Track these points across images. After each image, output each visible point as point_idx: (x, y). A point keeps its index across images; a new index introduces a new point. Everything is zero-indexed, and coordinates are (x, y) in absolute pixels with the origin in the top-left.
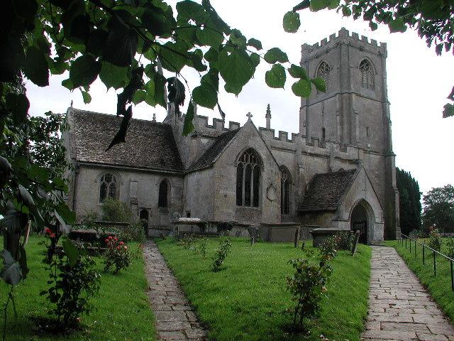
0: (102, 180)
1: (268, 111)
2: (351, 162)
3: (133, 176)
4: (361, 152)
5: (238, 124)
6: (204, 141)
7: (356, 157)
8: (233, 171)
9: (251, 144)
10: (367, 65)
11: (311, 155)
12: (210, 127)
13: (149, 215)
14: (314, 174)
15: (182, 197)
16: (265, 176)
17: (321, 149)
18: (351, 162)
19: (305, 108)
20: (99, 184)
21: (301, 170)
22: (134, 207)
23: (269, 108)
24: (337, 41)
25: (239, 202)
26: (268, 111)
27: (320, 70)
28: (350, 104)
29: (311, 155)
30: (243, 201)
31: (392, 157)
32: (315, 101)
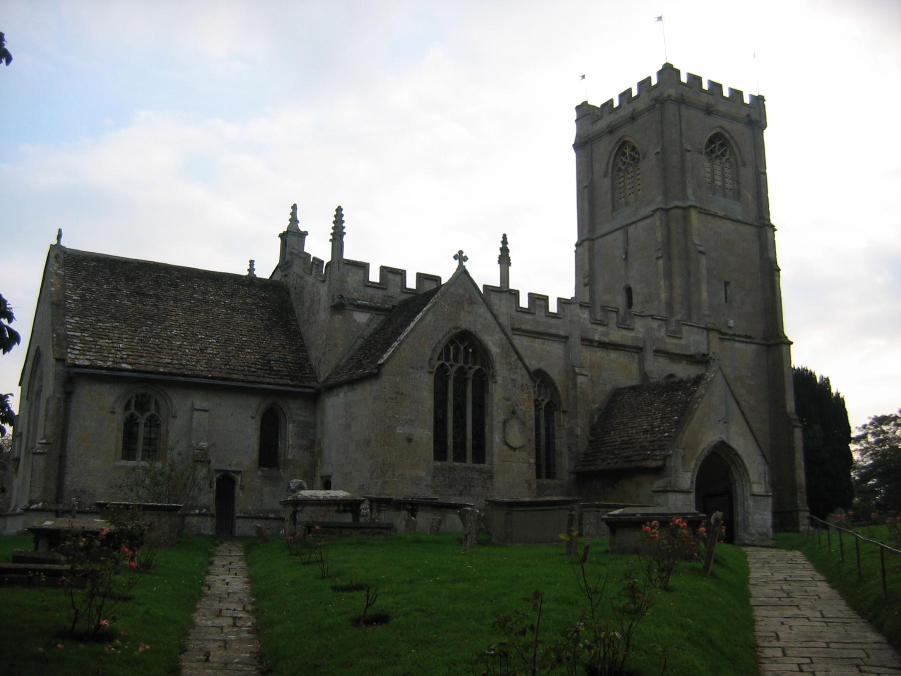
0: (127, 407)
1: (505, 251)
2: (692, 359)
3: (200, 401)
4: (714, 336)
5: (437, 279)
6: (361, 317)
7: (703, 349)
8: (426, 381)
9: (466, 322)
10: (722, 145)
11: (603, 345)
12: (373, 285)
13: (238, 487)
14: (608, 388)
15: (313, 447)
16: (497, 393)
17: (625, 332)
18: (692, 359)
19: (586, 244)
20: (119, 418)
21: (580, 379)
22: (202, 472)
23: (505, 241)
24: (654, 94)
25: (440, 453)
26: (505, 251)
27: (618, 160)
28: (686, 232)
29: (603, 345)
30: (450, 451)
31: (784, 347)
32: (608, 228)
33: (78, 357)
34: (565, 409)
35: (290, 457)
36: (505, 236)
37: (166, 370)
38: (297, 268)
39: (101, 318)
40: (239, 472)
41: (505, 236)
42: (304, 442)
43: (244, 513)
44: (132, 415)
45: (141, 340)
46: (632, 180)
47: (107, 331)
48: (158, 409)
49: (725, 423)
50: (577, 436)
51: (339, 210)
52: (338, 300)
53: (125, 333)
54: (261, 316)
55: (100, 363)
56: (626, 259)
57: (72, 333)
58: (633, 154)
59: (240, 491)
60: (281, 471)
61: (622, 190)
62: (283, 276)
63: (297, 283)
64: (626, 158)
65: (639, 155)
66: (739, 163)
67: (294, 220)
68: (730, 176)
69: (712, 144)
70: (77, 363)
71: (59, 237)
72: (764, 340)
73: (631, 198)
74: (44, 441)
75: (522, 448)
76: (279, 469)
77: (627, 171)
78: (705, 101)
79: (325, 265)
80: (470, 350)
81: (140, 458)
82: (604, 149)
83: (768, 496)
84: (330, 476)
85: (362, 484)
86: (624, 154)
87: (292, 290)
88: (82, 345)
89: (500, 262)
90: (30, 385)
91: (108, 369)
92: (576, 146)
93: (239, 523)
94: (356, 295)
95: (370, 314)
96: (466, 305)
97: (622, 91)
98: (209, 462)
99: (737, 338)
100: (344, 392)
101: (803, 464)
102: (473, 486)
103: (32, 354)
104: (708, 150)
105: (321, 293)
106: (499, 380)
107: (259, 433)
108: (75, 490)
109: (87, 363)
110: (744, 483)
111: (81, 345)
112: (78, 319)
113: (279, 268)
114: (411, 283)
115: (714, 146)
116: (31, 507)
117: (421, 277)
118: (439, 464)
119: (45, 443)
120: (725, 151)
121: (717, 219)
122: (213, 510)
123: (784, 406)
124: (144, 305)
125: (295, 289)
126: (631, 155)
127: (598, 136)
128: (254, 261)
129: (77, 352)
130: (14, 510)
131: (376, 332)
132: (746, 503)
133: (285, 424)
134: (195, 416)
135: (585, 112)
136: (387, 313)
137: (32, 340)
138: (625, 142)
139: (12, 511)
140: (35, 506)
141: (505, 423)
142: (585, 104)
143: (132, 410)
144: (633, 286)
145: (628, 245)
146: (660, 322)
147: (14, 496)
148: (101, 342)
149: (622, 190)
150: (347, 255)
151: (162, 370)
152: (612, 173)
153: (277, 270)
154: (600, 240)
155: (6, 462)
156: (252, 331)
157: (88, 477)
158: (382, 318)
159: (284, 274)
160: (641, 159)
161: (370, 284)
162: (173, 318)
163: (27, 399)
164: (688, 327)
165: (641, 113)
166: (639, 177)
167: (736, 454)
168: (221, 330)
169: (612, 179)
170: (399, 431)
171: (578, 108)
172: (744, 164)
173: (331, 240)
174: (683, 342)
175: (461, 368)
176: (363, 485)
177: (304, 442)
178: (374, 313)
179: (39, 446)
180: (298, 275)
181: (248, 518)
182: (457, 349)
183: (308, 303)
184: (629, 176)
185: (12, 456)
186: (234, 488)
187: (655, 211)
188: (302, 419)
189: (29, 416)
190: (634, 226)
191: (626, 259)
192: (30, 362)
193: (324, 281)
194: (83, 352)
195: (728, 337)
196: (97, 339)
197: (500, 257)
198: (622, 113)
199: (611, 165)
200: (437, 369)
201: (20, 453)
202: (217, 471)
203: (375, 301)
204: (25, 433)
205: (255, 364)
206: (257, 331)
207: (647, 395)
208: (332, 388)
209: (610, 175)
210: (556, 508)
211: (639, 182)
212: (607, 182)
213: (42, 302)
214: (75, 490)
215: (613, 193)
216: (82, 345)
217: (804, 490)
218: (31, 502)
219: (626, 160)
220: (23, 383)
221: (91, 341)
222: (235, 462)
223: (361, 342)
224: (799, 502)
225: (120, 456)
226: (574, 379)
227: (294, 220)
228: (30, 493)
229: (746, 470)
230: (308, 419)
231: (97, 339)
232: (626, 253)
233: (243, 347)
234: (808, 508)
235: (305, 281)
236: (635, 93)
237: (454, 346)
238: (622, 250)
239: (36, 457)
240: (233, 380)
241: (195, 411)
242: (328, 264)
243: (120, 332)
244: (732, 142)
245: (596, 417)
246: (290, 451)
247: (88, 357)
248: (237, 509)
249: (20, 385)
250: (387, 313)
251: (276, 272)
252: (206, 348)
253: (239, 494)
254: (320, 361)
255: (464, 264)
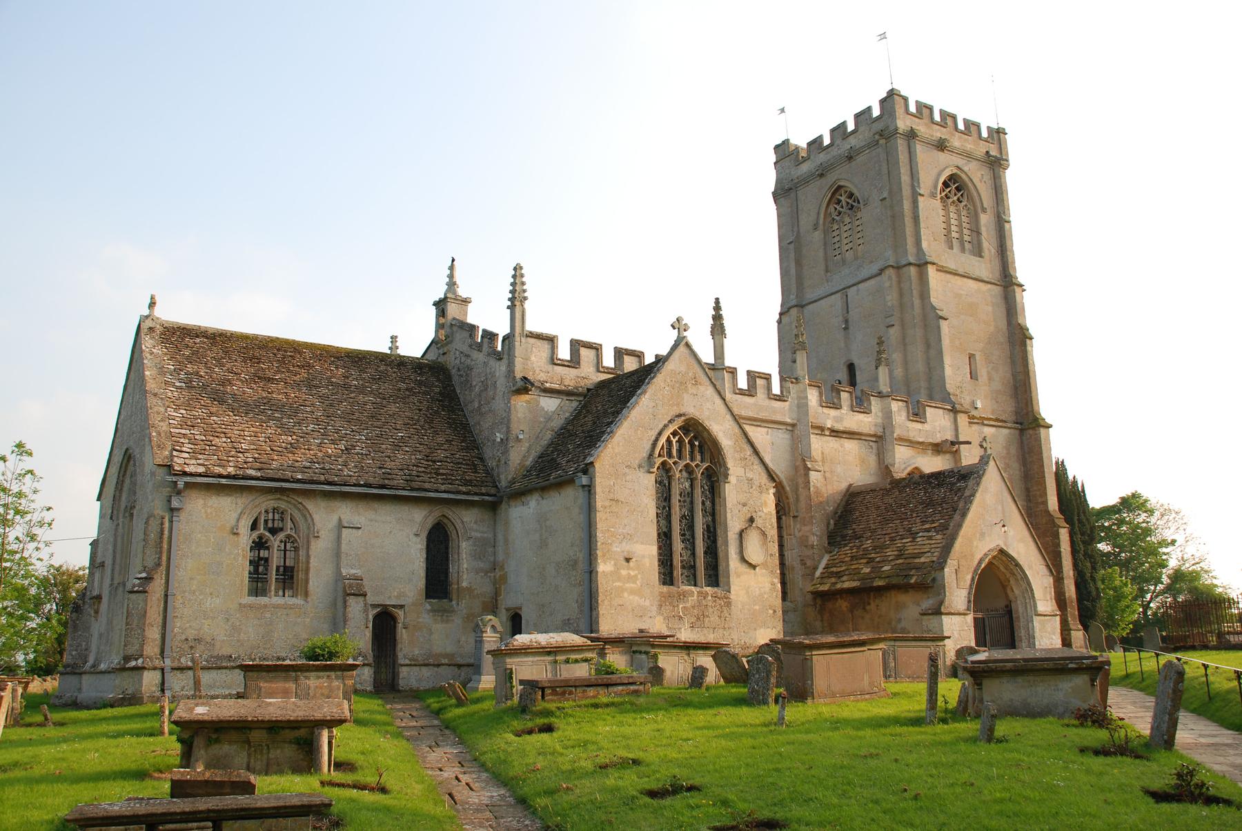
0: (254, 527)
1: (717, 318)
2: (937, 448)
3: (346, 511)
4: (962, 419)
5: (639, 355)
6: (550, 404)
7: (949, 436)
8: (646, 484)
9: (691, 408)
10: (958, 189)
11: (835, 433)
12: (563, 364)
13: (400, 625)
14: (843, 486)
15: (496, 572)
16: (732, 492)
17: (861, 416)
18: (937, 448)
19: (794, 311)
20: (246, 538)
21: (813, 475)
22: (355, 606)
23: (717, 307)
24: (878, 126)
25: (667, 577)
26: (717, 318)
27: (831, 208)
28: (924, 294)
29: (835, 433)
30: (678, 572)
31: (1042, 431)
32: (820, 292)
33: (187, 461)
34: (796, 514)
35: (464, 584)
36: (717, 301)
37: (306, 476)
38: (460, 343)
39: (214, 410)
40: (402, 607)
41: (717, 301)
42: (482, 565)
43: (410, 660)
44: (260, 537)
45: (269, 438)
46: (849, 233)
47: (223, 426)
48: (295, 526)
49: (1004, 526)
50: (812, 547)
51: (517, 268)
52: (522, 383)
53: (247, 429)
54: (419, 404)
55: (218, 470)
56: (846, 328)
57: (177, 431)
58: (850, 201)
59: (404, 630)
60: (454, 602)
61: (837, 246)
62: (439, 354)
63: (461, 363)
64: (842, 207)
65: (859, 202)
66: (979, 210)
67: (452, 284)
68: (968, 226)
69: (947, 188)
70: (187, 470)
71: (152, 304)
72: (1017, 423)
73: (849, 256)
74: (144, 575)
75: (765, 565)
76: (451, 600)
77: (843, 222)
78: (939, 135)
79: (500, 339)
80: (697, 443)
81: (273, 593)
82: (813, 199)
83: (1057, 615)
84: (520, 609)
85: (567, 618)
86: (839, 202)
87: (454, 372)
88: (192, 447)
89: (713, 333)
90: (116, 499)
91: (228, 477)
92: (776, 195)
93: (404, 671)
94: (542, 377)
95: (560, 400)
96: (690, 386)
97: (835, 125)
98: (365, 595)
99: (985, 422)
100: (537, 500)
101: (1071, 573)
102: (707, 616)
103: (118, 458)
104: (943, 194)
105: (497, 375)
106: (732, 479)
107: (425, 556)
108: (187, 640)
109: (201, 470)
110: (1027, 601)
111: (190, 446)
112: (184, 412)
113: (434, 344)
114: (609, 361)
115: (949, 189)
116: (127, 666)
117: (620, 353)
118: (665, 589)
119: (145, 578)
120: (962, 195)
121: (956, 277)
122: (371, 660)
123: (1045, 503)
124: (269, 393)
125: (459, 370)
126: (848, 203)
127: (805, 181)
128: (396, 337)
129: (186, 455)
130: (94, 666)
131: (570, 422)
132: (1030, 625)
133: (457, 543)
134: (343, 536)
135: (784, 152)
136: (581, 399)
137: (117, 440)
138: (840, 187)
139: (91, 668)
140: (133, 663)
141: (741, 534)
142: (786, 143)
143: (261, 530)
144: (856, 362)
145: (848, 312)
146: (900, 403)
147: (94, 648)
148: (216, 441)
149: (837, 246)
150: (531, 326)
151: (300, 477)
152: (824, 224)
153: (432, 347)
154: (810, 307)
155: (80, 602)
156: (408, 424)
157: (204, 621)
158: (575, 404)
159: (441, 351)
160: (862, 207)
161: (559, 362)
162: (308, 409)
163: (111, 518)
164: (932, 409)
165: (859, 151)
166: (859, 229)
167: (1017, 565)
168: (370, 423)
169: (825, 232)
170: (615, 549)
171: (777, 148)
172: (984, 210)
173: (508, 307)
174: (926, 427)
175: (687, 466)
176: (568, 620)
177: (482, 565)
178: (565, 398)
179: (137, 582)
180: (462, 353)
181: (415, 665)
182: (680, 441)
183: (477, 387)
184: (846, 228)
185: (88, 593)
186: (395, 627)
187: (881, 271)
188: (479, 535)
189: (115, 540)
190: (855, 288)
191: (846, 328)
192: (114, 470)
193: (501, 359)
194: (194, 454)
195: (975, 421)
196: (211, 438)
197: (713, 327)
198: (834, 152)
199: (822, 216)
200: (658, 468)
201: (101, 588)
202: (374, 606)
203: (566, 384)
204: (108, 562)
205: (418, 466)
206: (415, 424)
207: (897, 493)
208: (520, 494)
209: (821, 227)
210: (865, 648)
211: (859, 235)
212: (818, 235)
213: (130, 390)
214: (187, 640)
215: (825, 249)
216: (192, 447)
217: (1075, 604)
218: (127, 659)
219: (841, 209)
220: (103, 496)
221: (203, 441)
222: (396, 593)
223: (550, 436)
224: (1069, 619)
225: (246, 591)
226: (807, 475)
227: (452, 284)
228: (125, 646)
229: (1029, 584)
230: (486, 535)
231: (211, 438)
232: (846, 321)
233: (401, 444)
234: (1080, 627)
235: (472, 360)
236: (851, 127)
237: (677, 438)
238: (841, 318)
239: (133, 596)
240: (426, 490)
241: (344, 529)
242: (505, 338)
243: (240, 428)
244: (970, 185)
245: (832, 522)
246: (465, 577)
247: (201, 462)
248: (400, 655)
249: (98, 499)
250: (581, 399)
251: (430, 349)
252: (354, 447)
253: (402, 634)
254: (499, 461)
255: (685, 334)
